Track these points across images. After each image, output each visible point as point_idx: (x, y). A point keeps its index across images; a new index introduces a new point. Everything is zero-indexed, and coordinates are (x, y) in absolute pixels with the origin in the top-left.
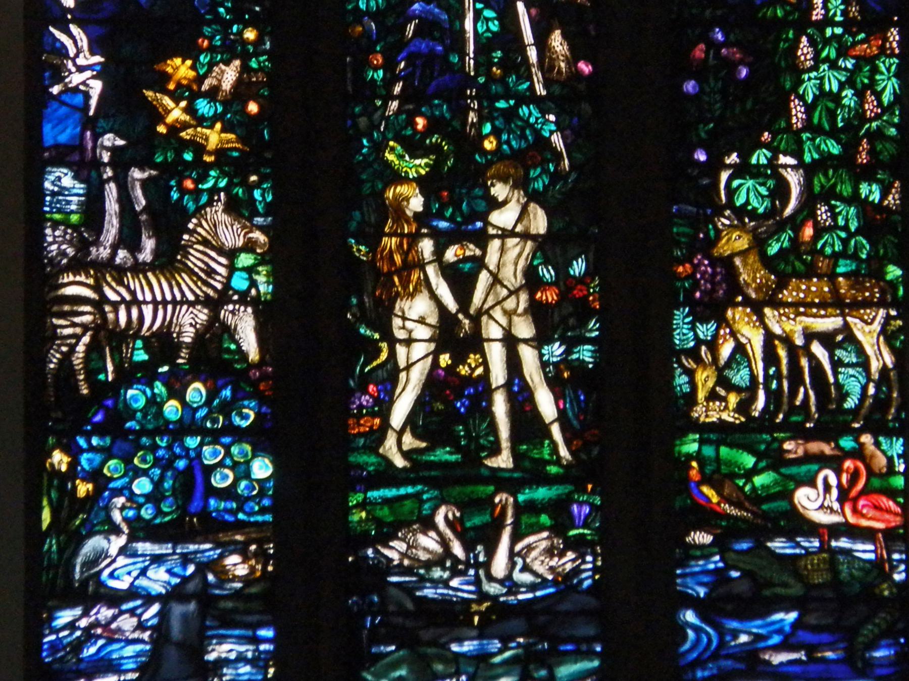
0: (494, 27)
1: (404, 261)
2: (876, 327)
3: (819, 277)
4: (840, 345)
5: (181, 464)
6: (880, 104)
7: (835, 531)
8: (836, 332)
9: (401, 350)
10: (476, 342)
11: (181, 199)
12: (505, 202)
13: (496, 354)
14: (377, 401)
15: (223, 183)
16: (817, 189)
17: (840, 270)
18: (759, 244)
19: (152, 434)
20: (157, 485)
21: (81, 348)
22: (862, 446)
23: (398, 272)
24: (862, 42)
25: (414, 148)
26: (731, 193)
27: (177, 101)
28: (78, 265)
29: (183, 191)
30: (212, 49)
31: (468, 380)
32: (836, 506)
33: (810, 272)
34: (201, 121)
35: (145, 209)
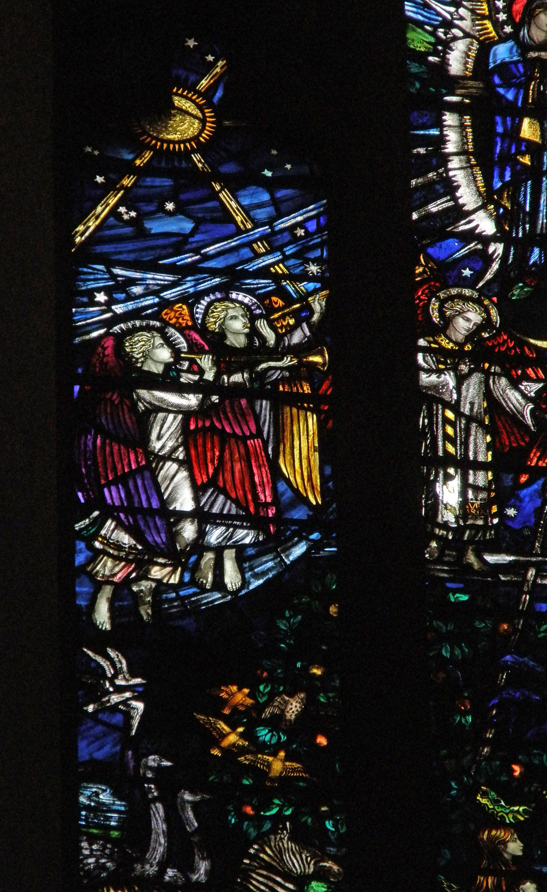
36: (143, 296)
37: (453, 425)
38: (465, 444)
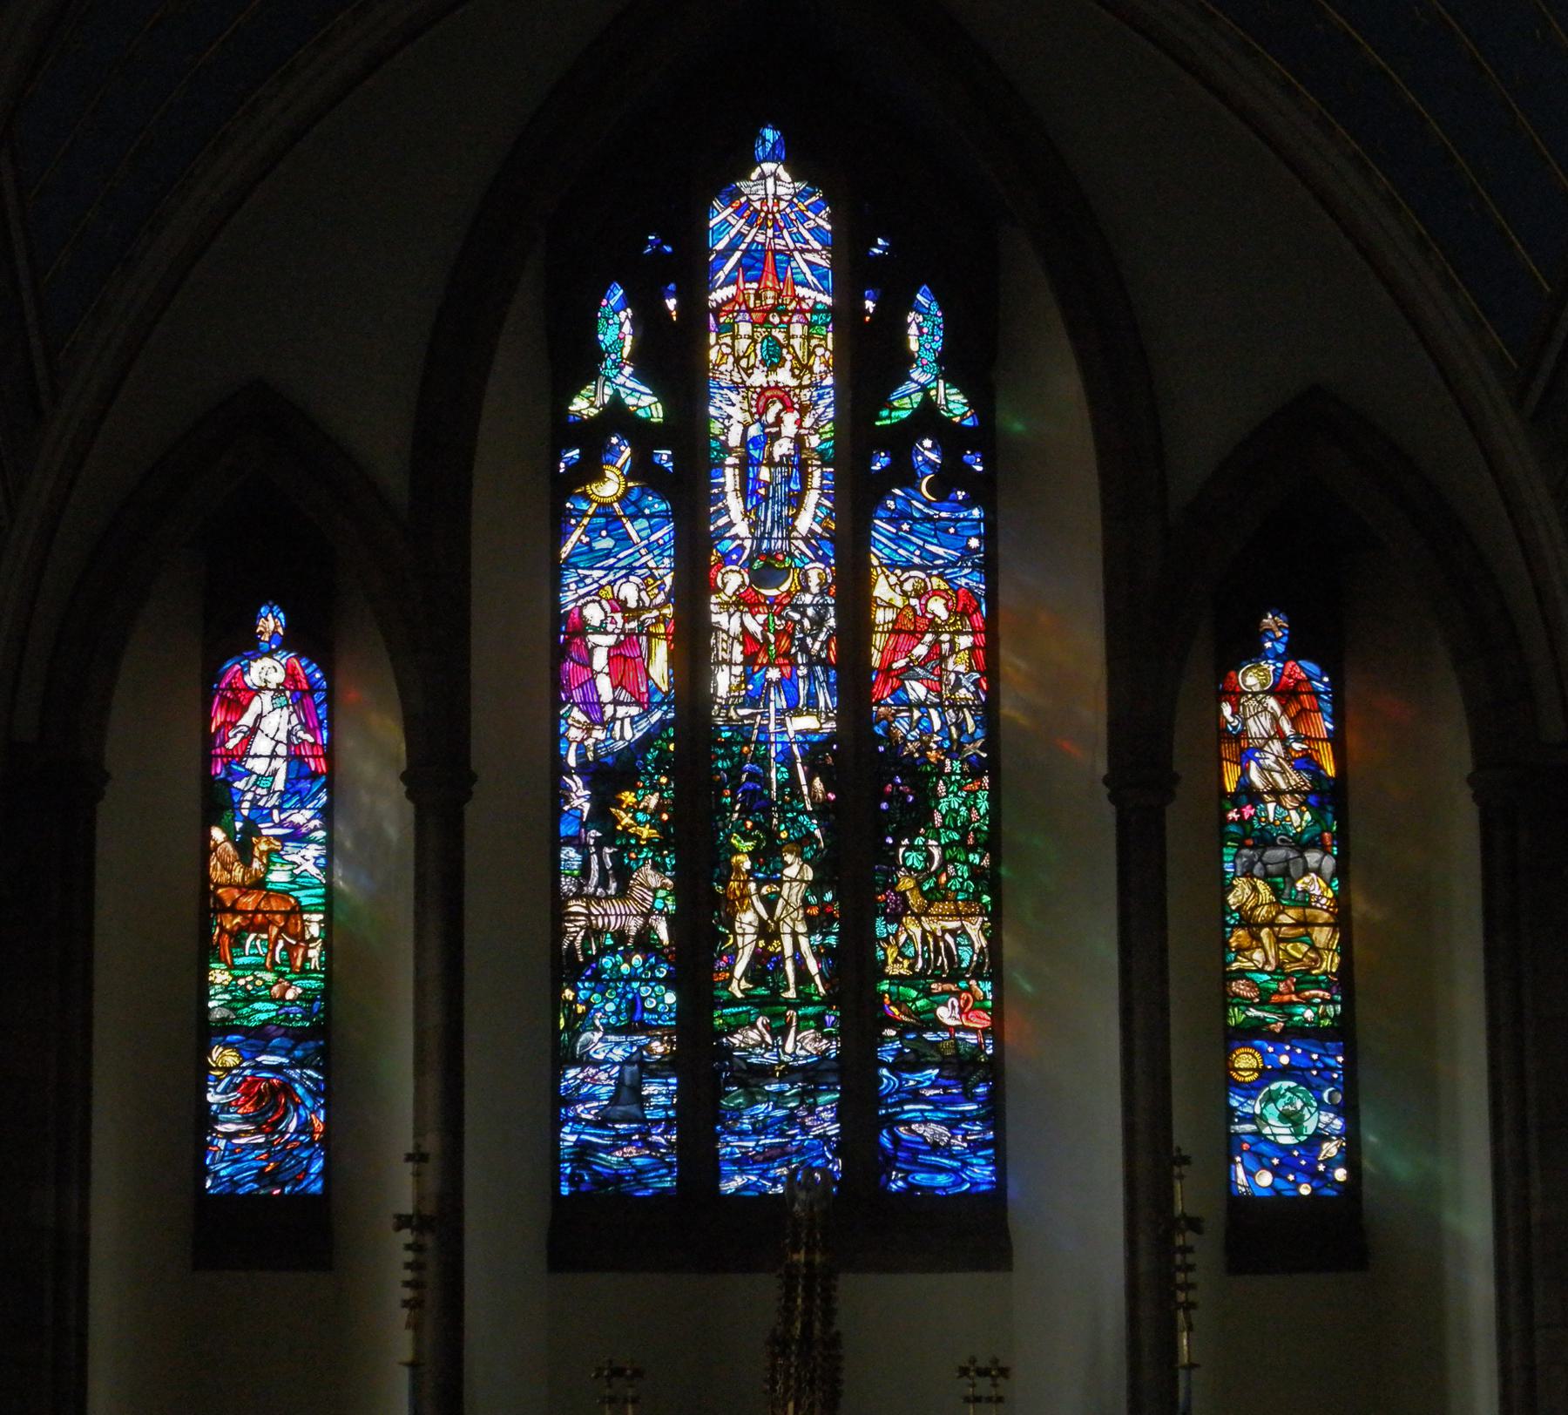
0: (786, 776)
1: (741, 894)
2: (978, 926)
3: (949, 901)
4: (959, 935)
5: (630, 996)
6: (979, 814)
7: (957, 1029)
8: (958, 929)
9: (740, 939)
10: (777, 935)
11: (629, 863)
12: (791, 864)
13: (787, 941)
14: (728, 964)
15: (650, 855)
16: (948, 857)
17: (959, 898)
18: (919, 885)
19: (615, 981)
20: (618, 1006)
21: (579, 938)
22: (970, 986)
23: (738, 899)
24: (970, 783)
25: (746, 836)
26: (904, 859)
27: (627, 813)
28: (577, 896)
29: (630, 859)
30: (644, 787)
31: (773, 954)
32: (958, 1016)
33: (944, 899)
34: (639, 823)
35: (611, 868)
36: (591, 584)
37: (726, 642)
38: (731, 652)
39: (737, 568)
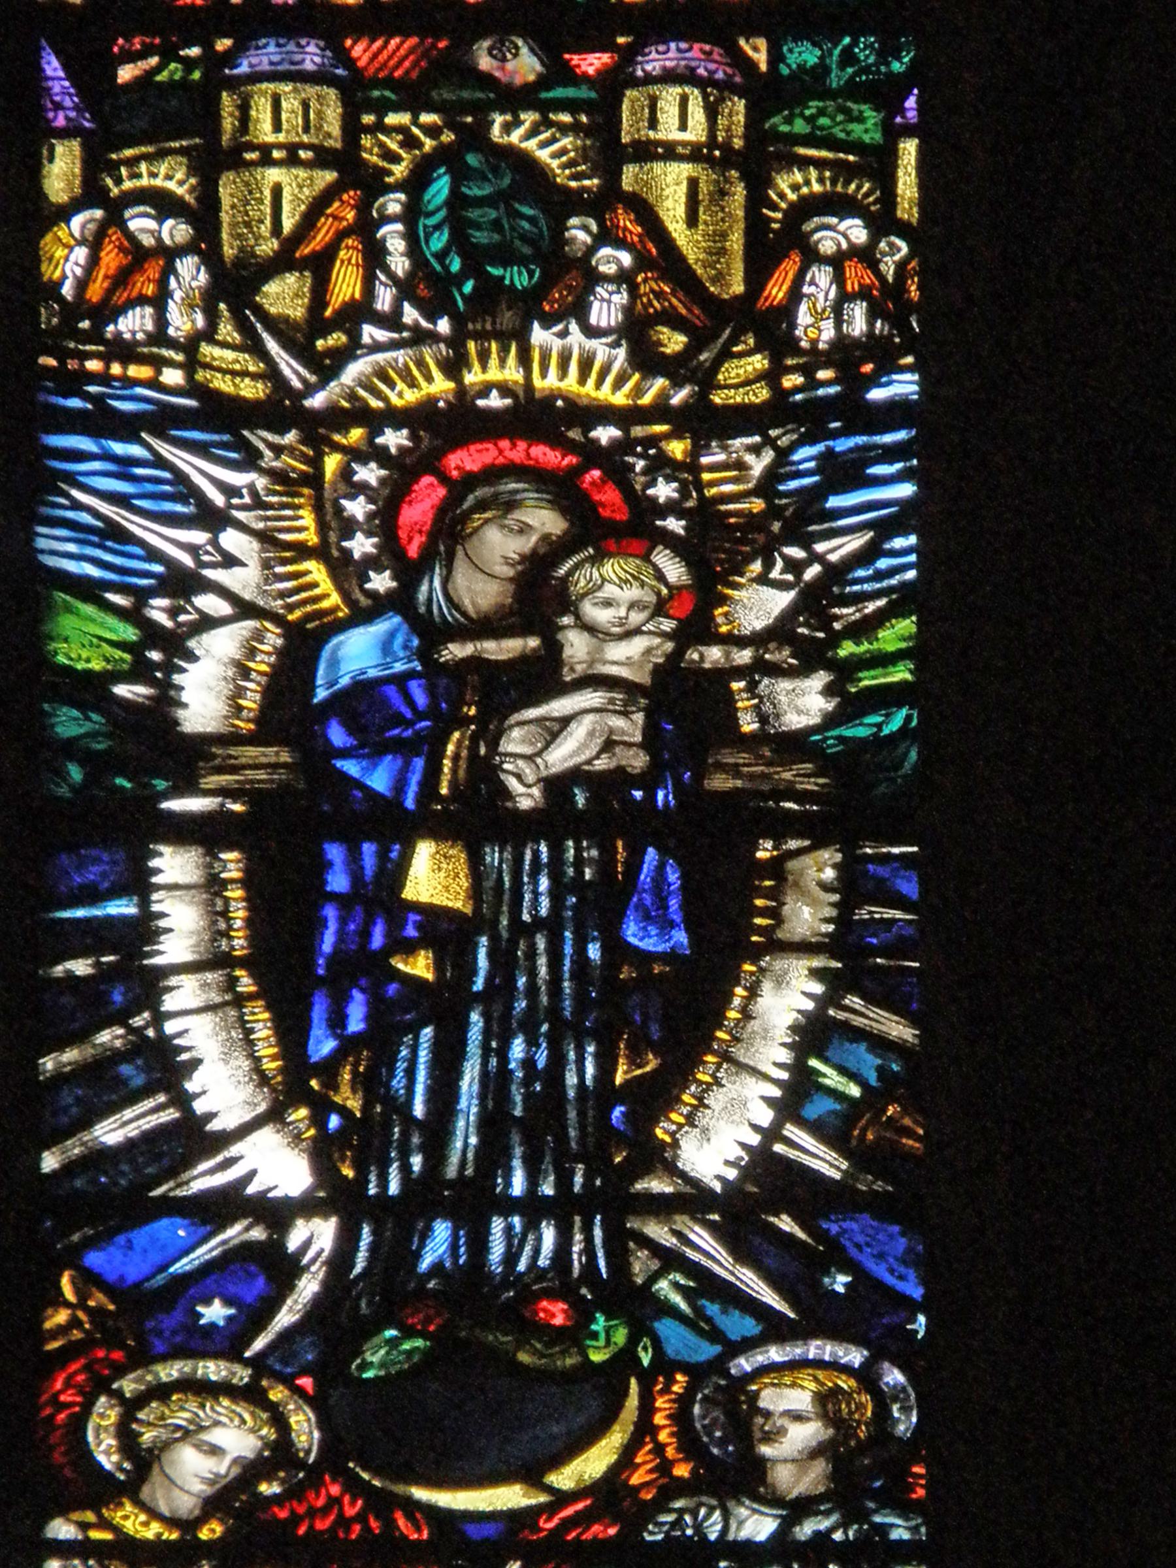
39: (242, 1375)
